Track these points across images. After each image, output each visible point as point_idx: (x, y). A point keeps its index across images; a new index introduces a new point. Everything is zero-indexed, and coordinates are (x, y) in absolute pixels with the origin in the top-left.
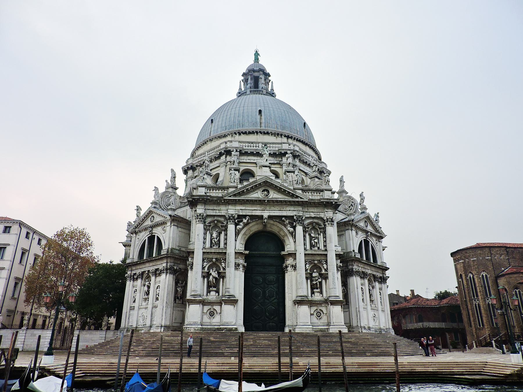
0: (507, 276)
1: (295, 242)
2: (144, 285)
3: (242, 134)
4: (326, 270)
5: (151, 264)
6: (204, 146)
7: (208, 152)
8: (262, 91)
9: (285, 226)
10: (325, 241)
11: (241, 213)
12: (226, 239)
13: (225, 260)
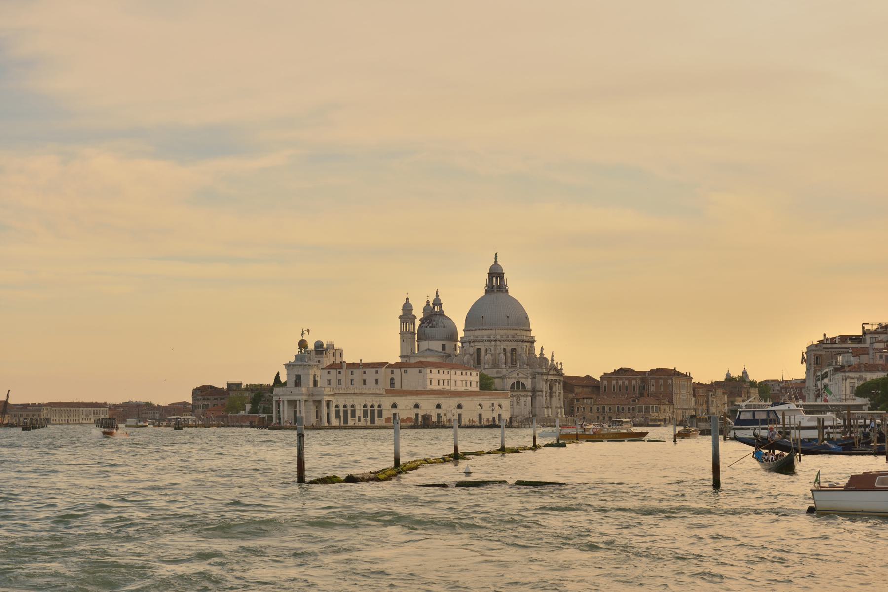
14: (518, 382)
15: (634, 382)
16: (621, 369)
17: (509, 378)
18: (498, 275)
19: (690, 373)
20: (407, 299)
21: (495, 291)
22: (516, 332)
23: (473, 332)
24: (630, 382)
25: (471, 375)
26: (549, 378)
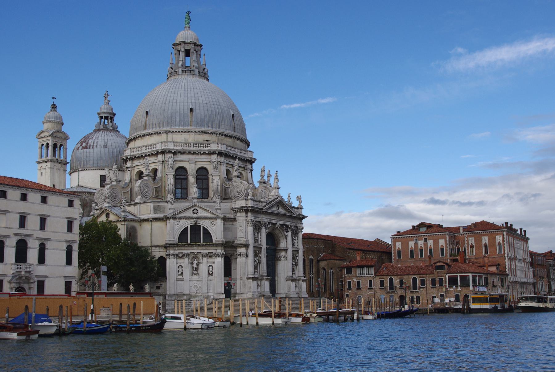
0: (328, 261)
1: (286, 242)
2: (192, 263)
3: (224, 136)
4: (298, 260)
5: (200, 248)
6: (183, 133)
7: (194, 144)
8: (206, 74)
9: (283, 230)
10: (298, 242)
11: (269, 221)
12: (260, 238)
13: (261, 252)
14: (195, 228)
15: (442, 242)
16: (422, 225)
17: (174, 219)
18: (187, 48)
19: (525, 231)
20: (54, 107)
21: (180, 72)
22: (207, 137)
23: (133, 142)
24: (436, 242)
25: (44, 200)
26: (265, 220)
